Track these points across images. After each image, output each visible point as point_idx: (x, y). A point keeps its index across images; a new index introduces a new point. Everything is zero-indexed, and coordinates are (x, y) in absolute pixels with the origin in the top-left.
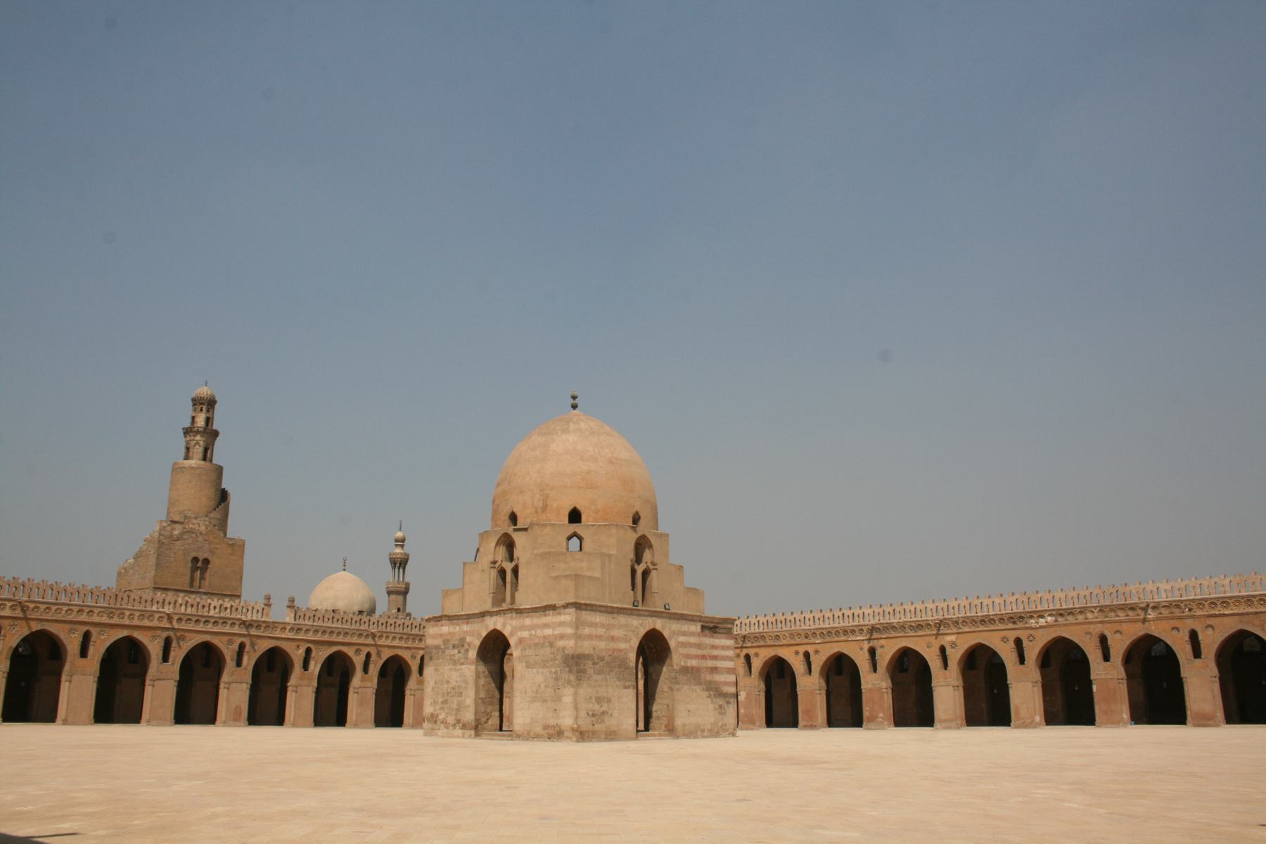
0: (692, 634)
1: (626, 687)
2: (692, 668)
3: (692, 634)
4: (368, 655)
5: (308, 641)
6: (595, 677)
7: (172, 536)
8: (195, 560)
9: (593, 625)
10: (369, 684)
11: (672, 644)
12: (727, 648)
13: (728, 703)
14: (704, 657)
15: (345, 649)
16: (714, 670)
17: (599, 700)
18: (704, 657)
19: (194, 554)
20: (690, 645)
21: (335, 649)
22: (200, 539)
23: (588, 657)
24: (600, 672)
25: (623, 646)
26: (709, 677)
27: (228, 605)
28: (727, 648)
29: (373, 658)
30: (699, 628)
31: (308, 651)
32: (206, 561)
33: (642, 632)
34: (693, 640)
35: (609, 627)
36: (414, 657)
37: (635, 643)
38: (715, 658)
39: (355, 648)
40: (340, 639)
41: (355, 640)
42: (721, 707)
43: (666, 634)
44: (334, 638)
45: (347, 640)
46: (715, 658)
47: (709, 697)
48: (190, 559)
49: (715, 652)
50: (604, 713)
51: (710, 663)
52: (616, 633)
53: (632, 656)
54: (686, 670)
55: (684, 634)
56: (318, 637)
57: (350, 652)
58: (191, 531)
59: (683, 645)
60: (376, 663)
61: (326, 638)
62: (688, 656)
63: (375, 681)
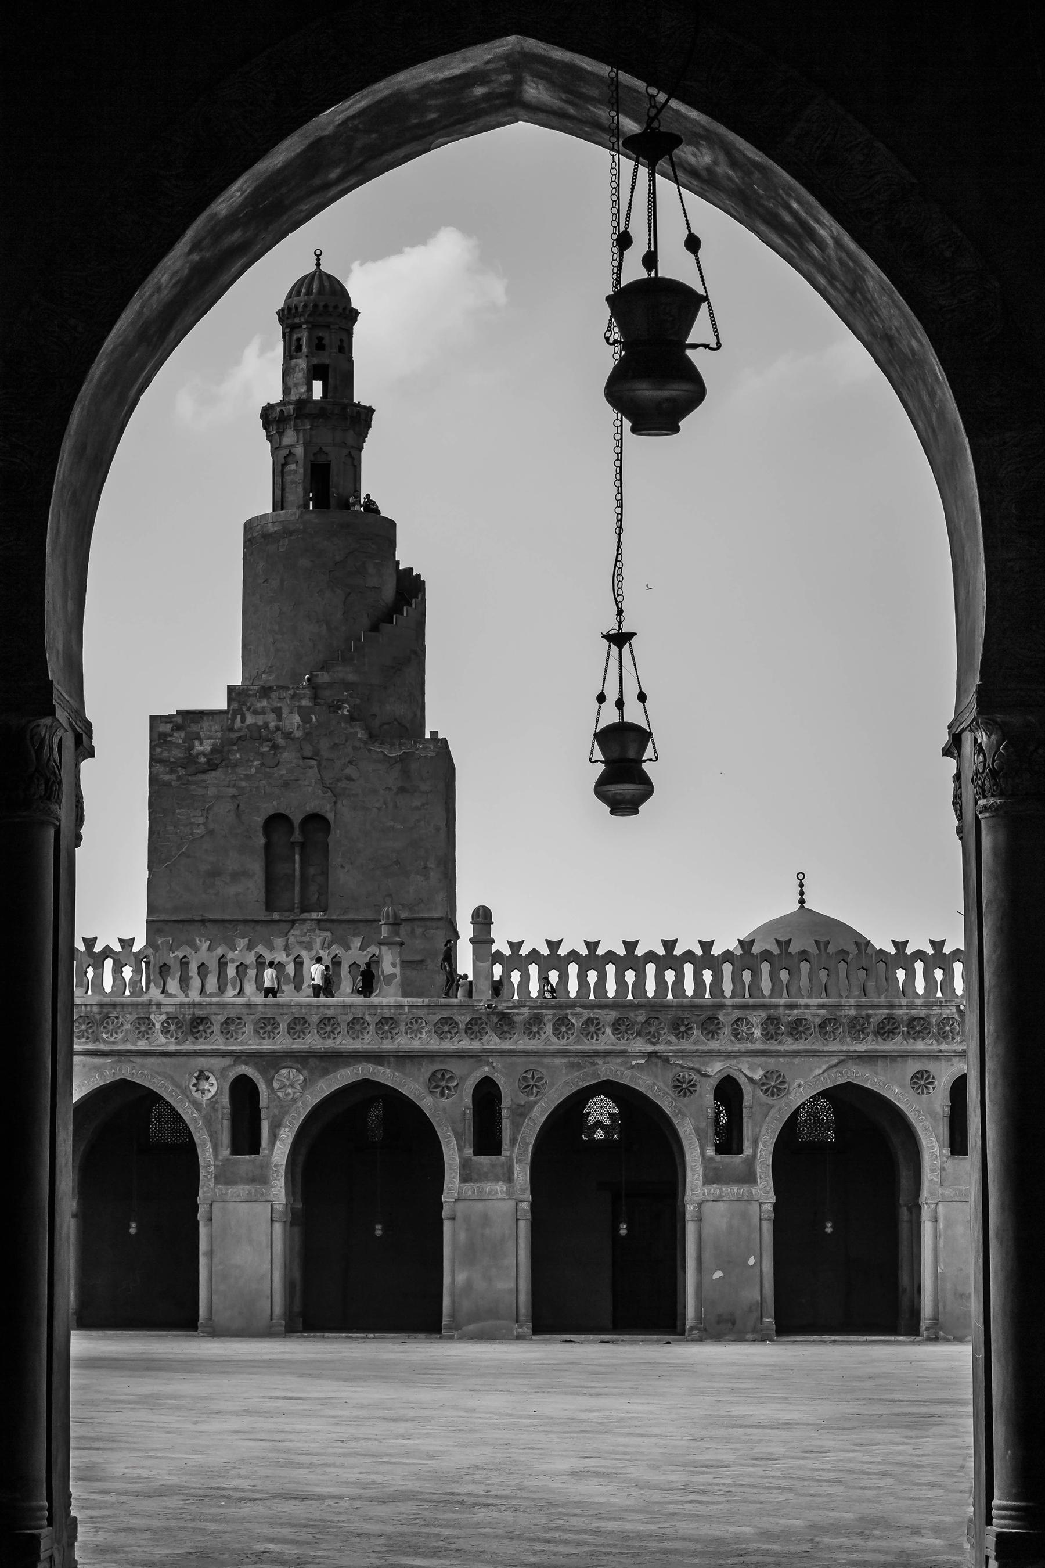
4: (487, 1095)
5: (239, 1057)
7: (190, 759)
8: (276, 822)
10: (500, 1188)
15: (385, 1075)
19: (270, 808)
21: (345, 1076)
22: (288, 756)
27: (250, 959)
31: (244, 1094)
32: (316, 822)
36: (683, 1088)
39: (427, 1069)
40: (368, 1042)
41: (426, 1041)
44: (344, 1043)
45: (403, 1042)
48: (259, 820)
56: (282, 1042)
57: (411, 1086)
58: (258, 735)
60: (521, 1112)
61: (312, 1041)
63: (522, 1174)
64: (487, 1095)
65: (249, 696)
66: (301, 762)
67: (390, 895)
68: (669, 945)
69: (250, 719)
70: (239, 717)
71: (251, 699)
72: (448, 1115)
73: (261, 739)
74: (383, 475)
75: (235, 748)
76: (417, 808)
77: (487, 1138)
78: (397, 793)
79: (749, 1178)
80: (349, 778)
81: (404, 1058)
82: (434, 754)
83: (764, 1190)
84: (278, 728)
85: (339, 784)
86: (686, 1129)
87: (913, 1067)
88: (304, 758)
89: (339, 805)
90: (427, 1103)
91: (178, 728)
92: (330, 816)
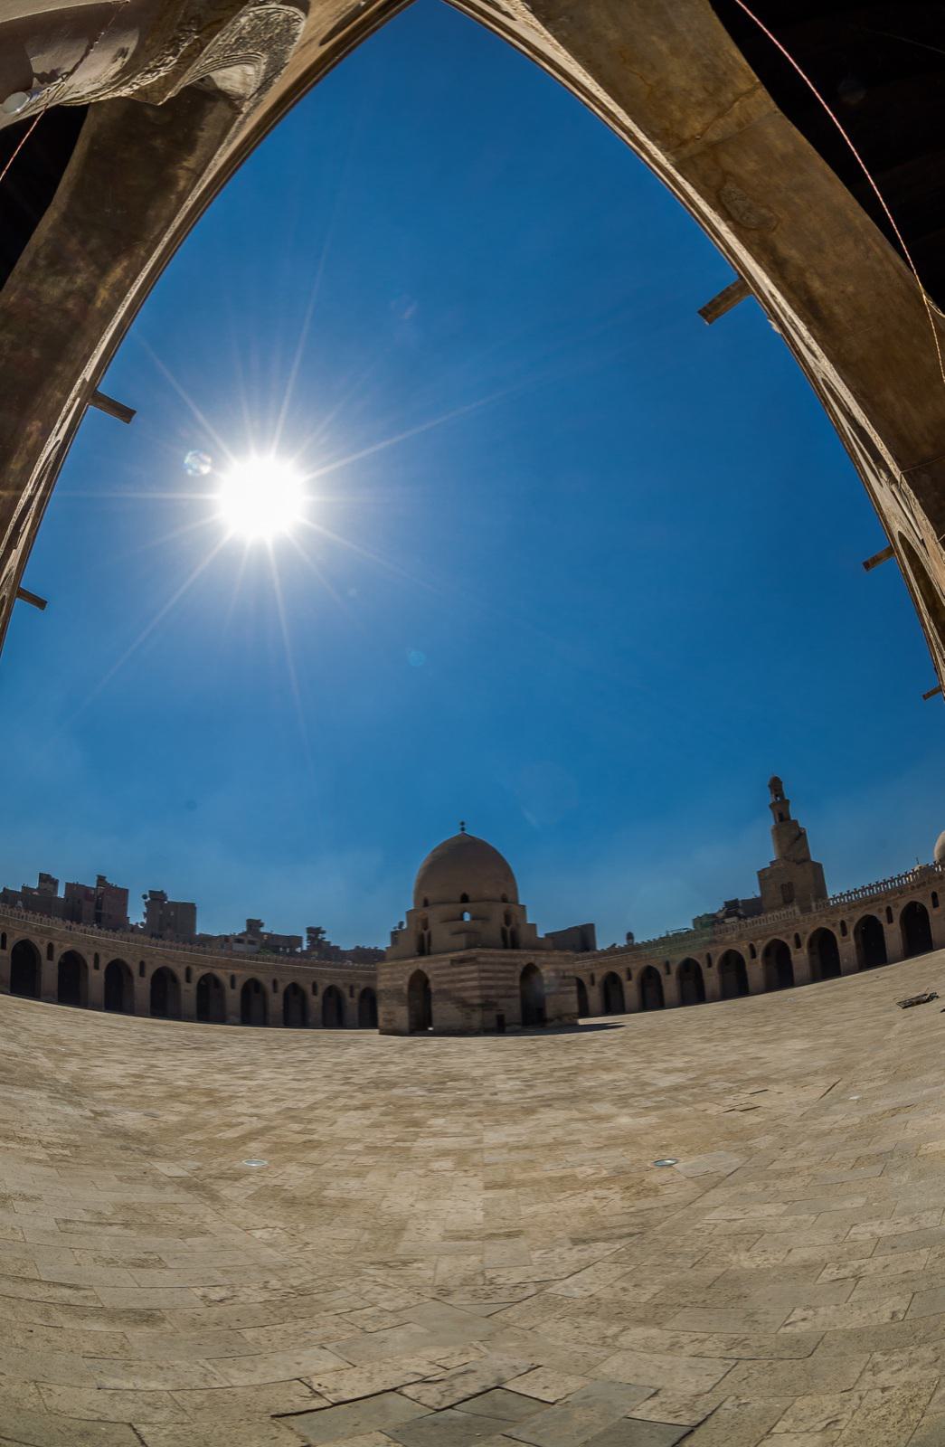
0: (443, 968)
1: (403, 1005)
2: (444, 990)
3: (443, 968)
4: (797, 936)
6: (387, 1001)
9: (385, 974)
11: (430, 977)
12: (472, 972)
13: (474, 1011)
14: (452, 981)
15: (777, 937)
16: (465, 989)
17: (389, 1013)
18: (452, 981)
20: (443, 975)
21: (770, 939)
23: (383, 991)
24: (388, 999)
25: (401, 982)
26: (457, 994)
28: (472, 972)
29: (847, 923)
30: (449, 963)
31: (751, 946)
33: (411, 972)
34: (444, 971)
35: (391, 973)
37: (407, 979)
38: (463, 981)
42: (467, 1014)
43: (425, 971)
46: (463, 981)
47: (457, 1008)
49: (463, 977)
50: (391, 1020)
51: (459, 985)
52: (396, 976)
53: (406, 988)
54: (440, 992)
55: (437, 969)
57: (782, 938)
59: (437, 976)
62: (441, 983)
64: (797, 936)
68: (841, 894)
72: (790, 943)
74: (794, 814)
77: (798, 945)
79: (850, 940)
81: (781, 933)
83: (852, 942)
86: (835, 933)
87: (877, 908)
90: (785, 941)
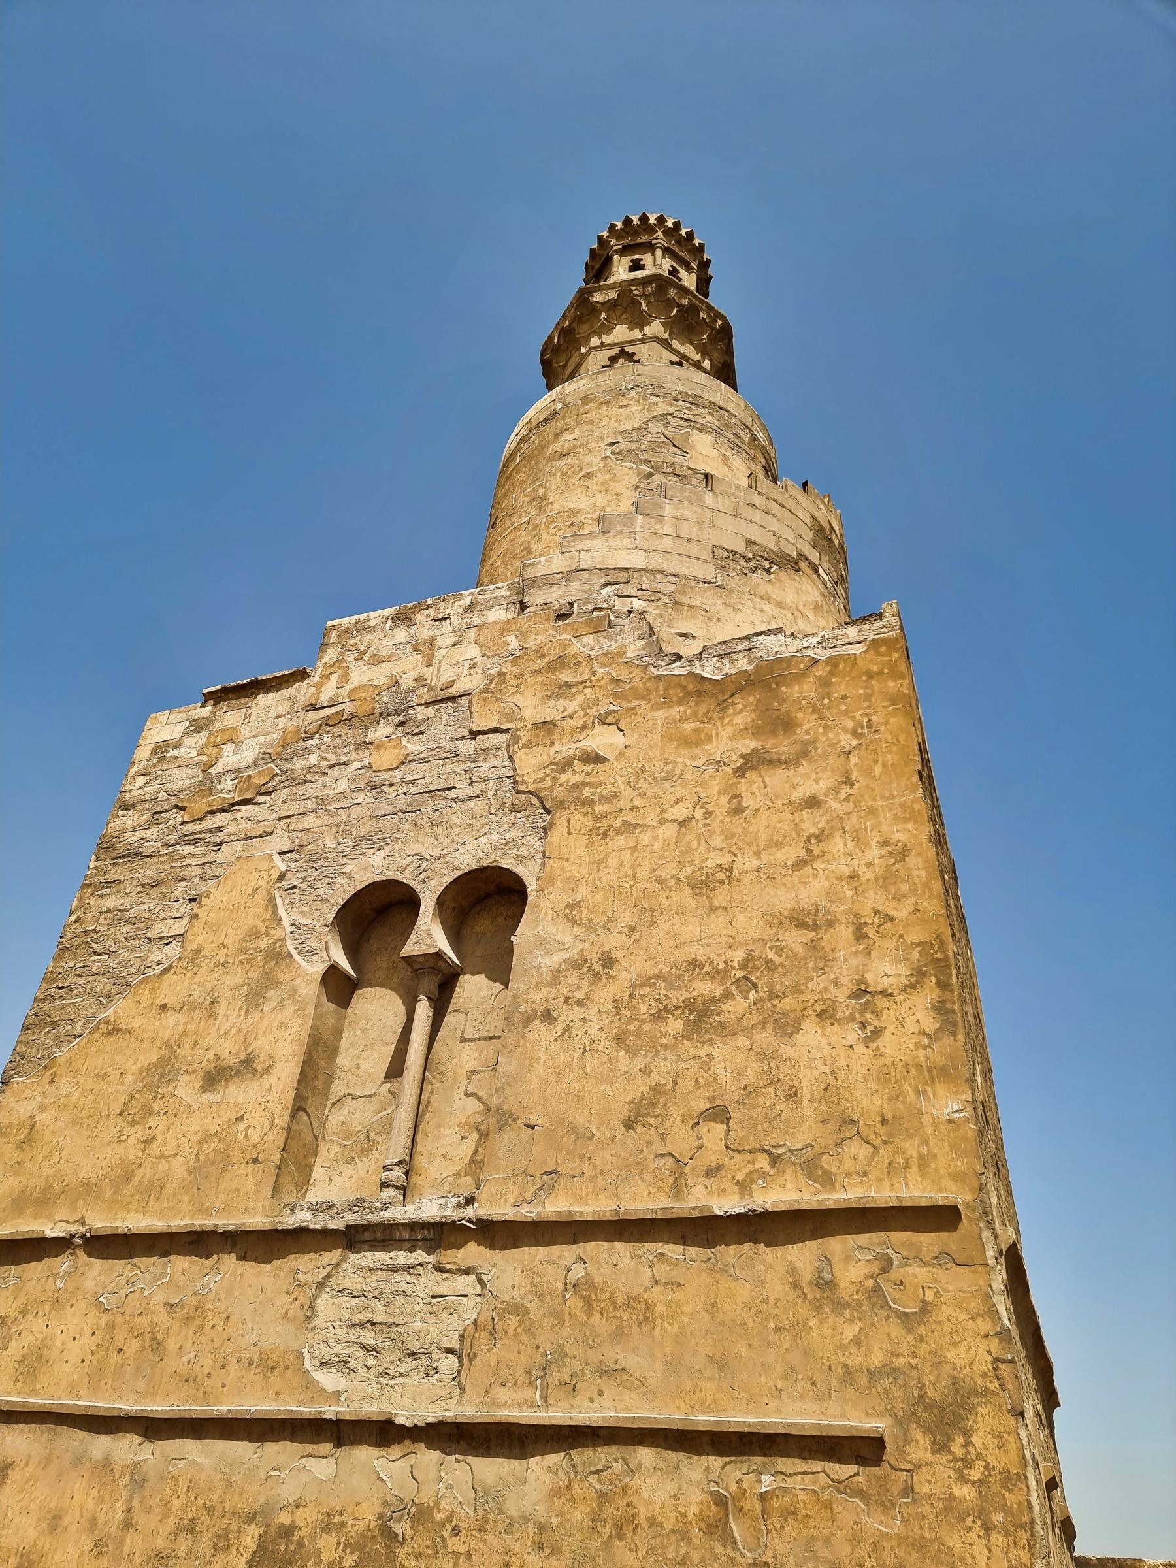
65: (371, 629)
66: (467, 747)
67: (719, 1114)
69: (359, 675)
70: (335, 678)
71: (370, 637)
73: (375, 716)
75: (315, 742)
76: (812, 803)
78: (741, 771)
80: (595, 759)
82: (859, 649)
84: (420, 680)
85: (563, 778)
88: (474, 734)
89: (556, 835)
91: (197, 725)
92: (528, 873)
